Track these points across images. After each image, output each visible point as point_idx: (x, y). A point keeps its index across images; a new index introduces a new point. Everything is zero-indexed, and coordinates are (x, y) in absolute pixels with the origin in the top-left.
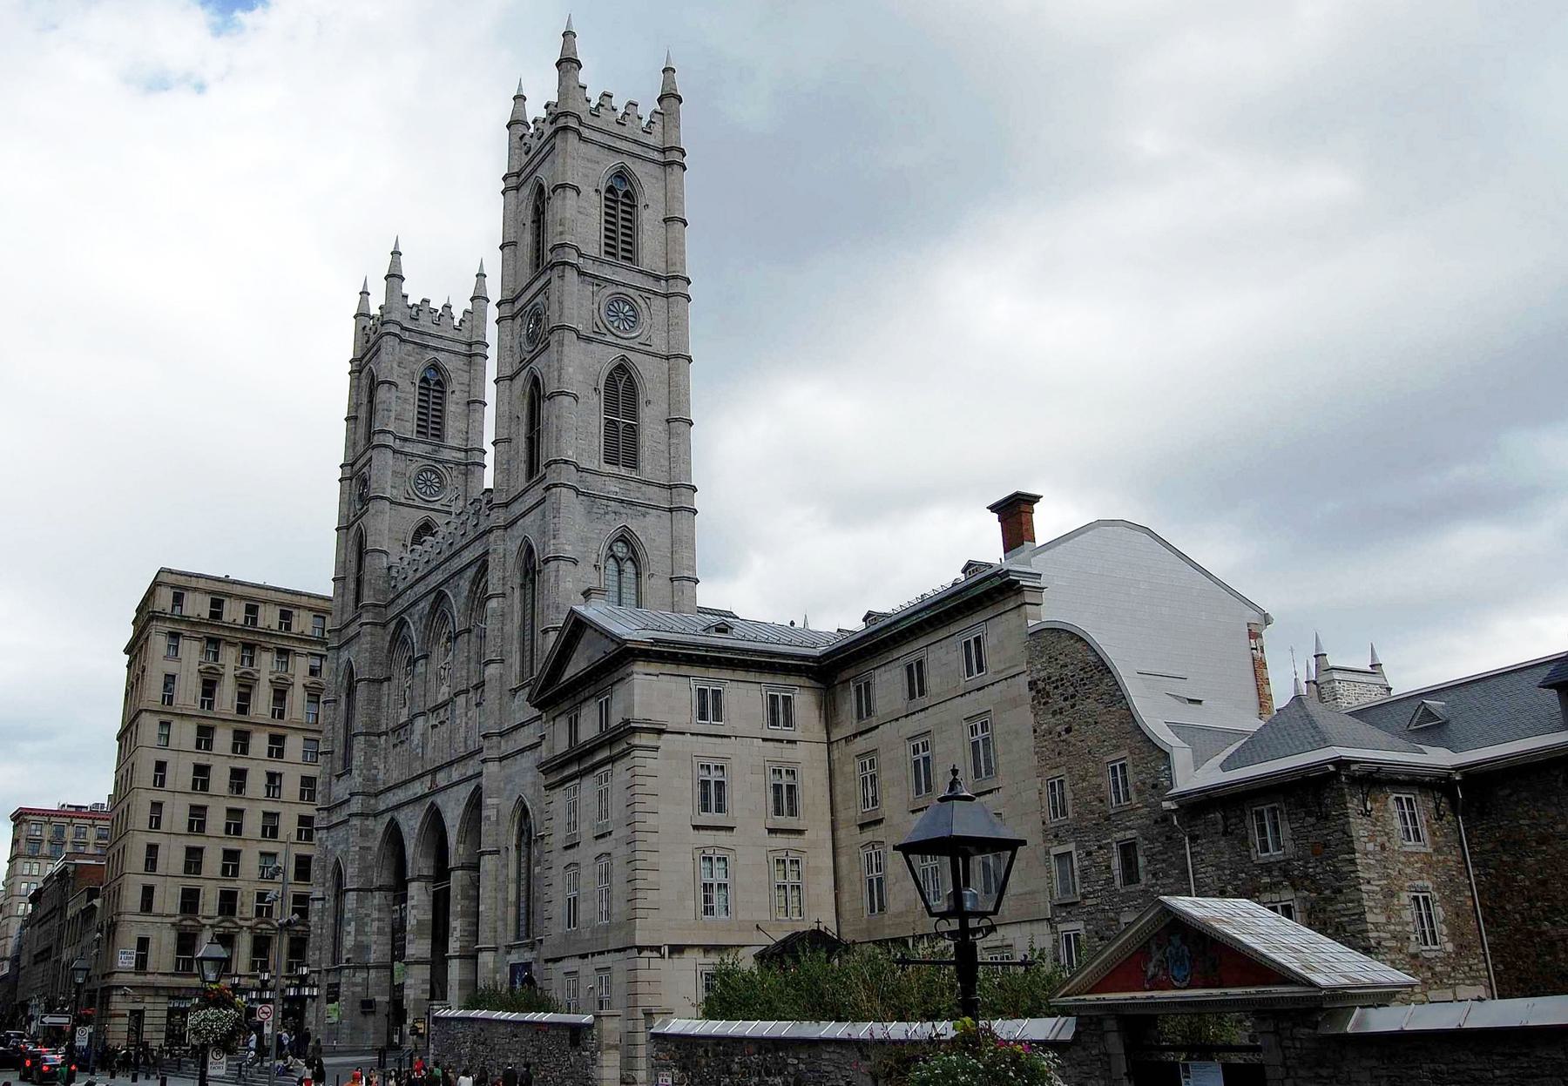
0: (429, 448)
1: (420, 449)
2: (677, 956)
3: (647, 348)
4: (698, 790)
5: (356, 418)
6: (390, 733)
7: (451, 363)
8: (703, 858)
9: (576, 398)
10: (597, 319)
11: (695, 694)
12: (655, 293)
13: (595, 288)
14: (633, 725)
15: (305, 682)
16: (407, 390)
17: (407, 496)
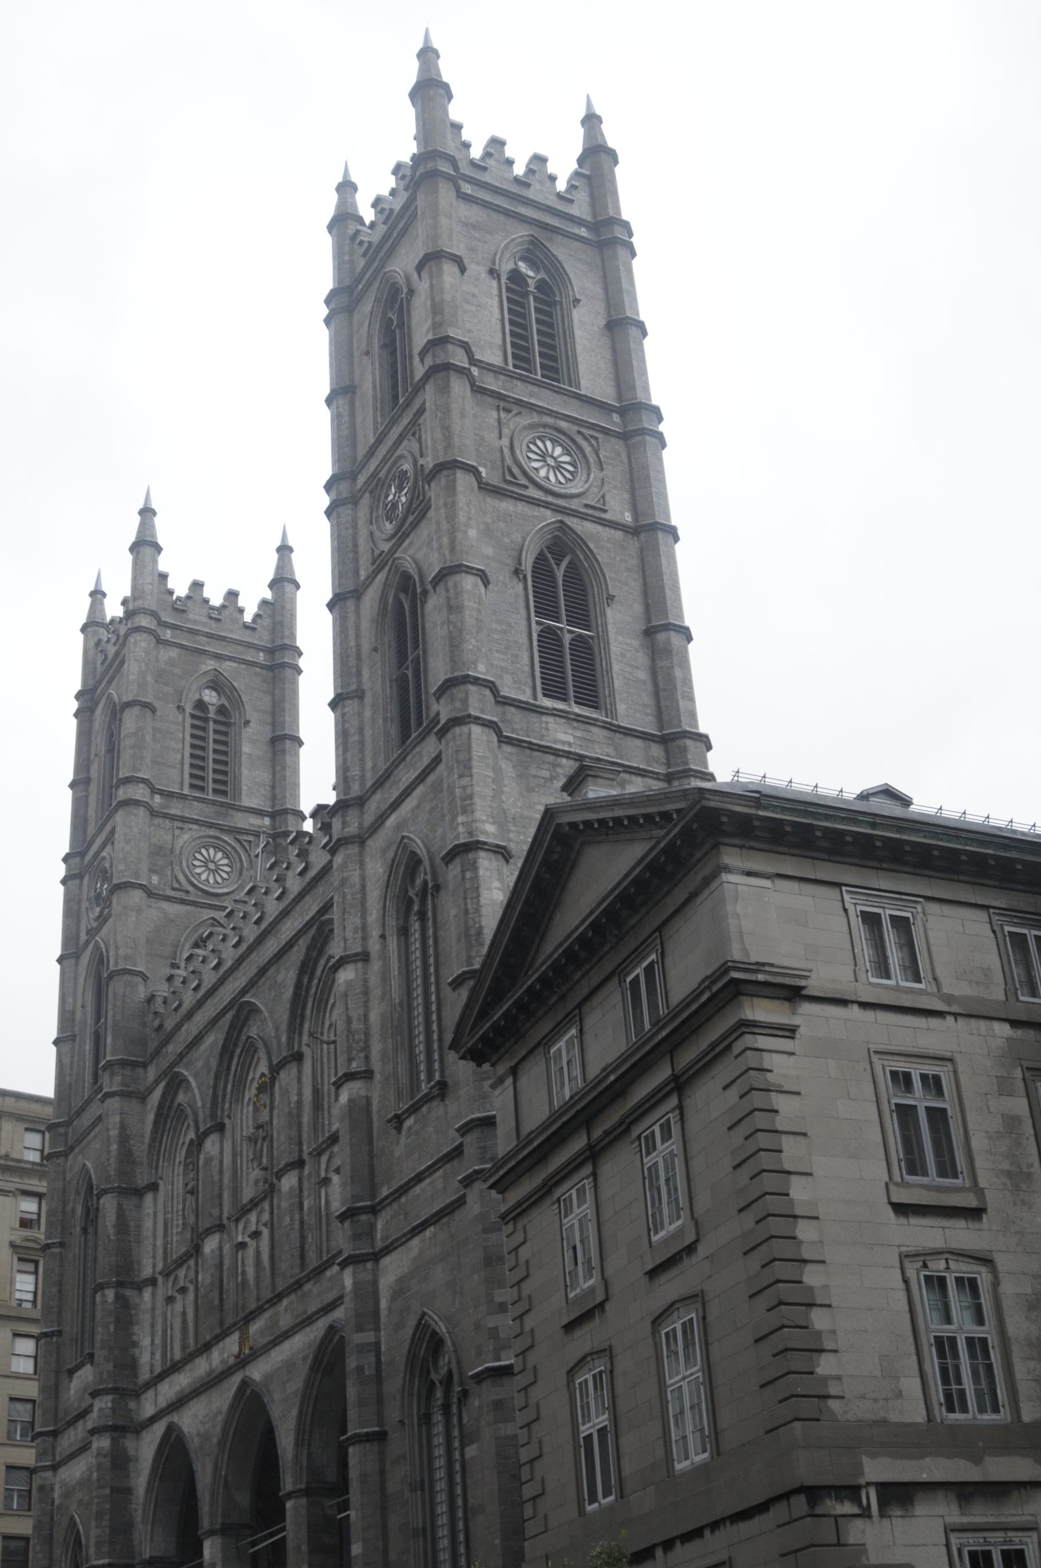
0: (209, 810)
1: (195, 811)
2: (899, 1513)
3: (597, 514)
4: (893, 1125)
5: (88, 781)
6: (160, 1280)
7: (243, 681)
8: (927, 1278)
9: (484, 577)
10: (509, 461)
11: (856, 922)
12: (605, 431)
13: (503, 415)
14: (735, 975)
15: (13, 1238)
16: (171, 718)
17: (176, 886)
